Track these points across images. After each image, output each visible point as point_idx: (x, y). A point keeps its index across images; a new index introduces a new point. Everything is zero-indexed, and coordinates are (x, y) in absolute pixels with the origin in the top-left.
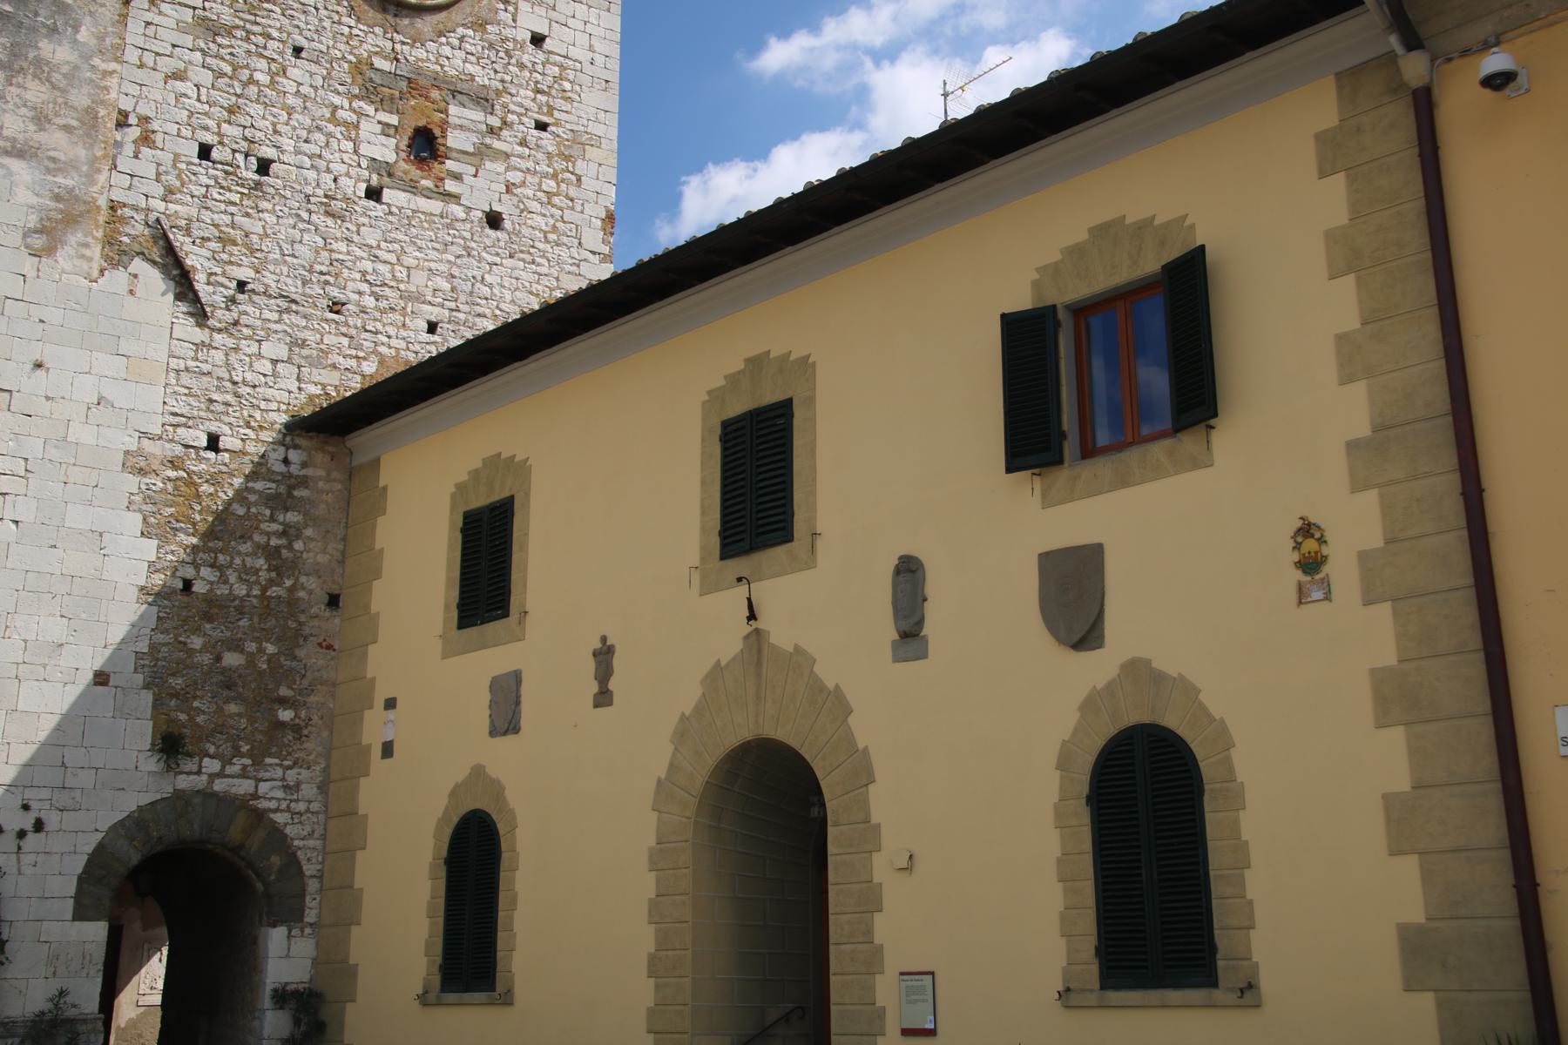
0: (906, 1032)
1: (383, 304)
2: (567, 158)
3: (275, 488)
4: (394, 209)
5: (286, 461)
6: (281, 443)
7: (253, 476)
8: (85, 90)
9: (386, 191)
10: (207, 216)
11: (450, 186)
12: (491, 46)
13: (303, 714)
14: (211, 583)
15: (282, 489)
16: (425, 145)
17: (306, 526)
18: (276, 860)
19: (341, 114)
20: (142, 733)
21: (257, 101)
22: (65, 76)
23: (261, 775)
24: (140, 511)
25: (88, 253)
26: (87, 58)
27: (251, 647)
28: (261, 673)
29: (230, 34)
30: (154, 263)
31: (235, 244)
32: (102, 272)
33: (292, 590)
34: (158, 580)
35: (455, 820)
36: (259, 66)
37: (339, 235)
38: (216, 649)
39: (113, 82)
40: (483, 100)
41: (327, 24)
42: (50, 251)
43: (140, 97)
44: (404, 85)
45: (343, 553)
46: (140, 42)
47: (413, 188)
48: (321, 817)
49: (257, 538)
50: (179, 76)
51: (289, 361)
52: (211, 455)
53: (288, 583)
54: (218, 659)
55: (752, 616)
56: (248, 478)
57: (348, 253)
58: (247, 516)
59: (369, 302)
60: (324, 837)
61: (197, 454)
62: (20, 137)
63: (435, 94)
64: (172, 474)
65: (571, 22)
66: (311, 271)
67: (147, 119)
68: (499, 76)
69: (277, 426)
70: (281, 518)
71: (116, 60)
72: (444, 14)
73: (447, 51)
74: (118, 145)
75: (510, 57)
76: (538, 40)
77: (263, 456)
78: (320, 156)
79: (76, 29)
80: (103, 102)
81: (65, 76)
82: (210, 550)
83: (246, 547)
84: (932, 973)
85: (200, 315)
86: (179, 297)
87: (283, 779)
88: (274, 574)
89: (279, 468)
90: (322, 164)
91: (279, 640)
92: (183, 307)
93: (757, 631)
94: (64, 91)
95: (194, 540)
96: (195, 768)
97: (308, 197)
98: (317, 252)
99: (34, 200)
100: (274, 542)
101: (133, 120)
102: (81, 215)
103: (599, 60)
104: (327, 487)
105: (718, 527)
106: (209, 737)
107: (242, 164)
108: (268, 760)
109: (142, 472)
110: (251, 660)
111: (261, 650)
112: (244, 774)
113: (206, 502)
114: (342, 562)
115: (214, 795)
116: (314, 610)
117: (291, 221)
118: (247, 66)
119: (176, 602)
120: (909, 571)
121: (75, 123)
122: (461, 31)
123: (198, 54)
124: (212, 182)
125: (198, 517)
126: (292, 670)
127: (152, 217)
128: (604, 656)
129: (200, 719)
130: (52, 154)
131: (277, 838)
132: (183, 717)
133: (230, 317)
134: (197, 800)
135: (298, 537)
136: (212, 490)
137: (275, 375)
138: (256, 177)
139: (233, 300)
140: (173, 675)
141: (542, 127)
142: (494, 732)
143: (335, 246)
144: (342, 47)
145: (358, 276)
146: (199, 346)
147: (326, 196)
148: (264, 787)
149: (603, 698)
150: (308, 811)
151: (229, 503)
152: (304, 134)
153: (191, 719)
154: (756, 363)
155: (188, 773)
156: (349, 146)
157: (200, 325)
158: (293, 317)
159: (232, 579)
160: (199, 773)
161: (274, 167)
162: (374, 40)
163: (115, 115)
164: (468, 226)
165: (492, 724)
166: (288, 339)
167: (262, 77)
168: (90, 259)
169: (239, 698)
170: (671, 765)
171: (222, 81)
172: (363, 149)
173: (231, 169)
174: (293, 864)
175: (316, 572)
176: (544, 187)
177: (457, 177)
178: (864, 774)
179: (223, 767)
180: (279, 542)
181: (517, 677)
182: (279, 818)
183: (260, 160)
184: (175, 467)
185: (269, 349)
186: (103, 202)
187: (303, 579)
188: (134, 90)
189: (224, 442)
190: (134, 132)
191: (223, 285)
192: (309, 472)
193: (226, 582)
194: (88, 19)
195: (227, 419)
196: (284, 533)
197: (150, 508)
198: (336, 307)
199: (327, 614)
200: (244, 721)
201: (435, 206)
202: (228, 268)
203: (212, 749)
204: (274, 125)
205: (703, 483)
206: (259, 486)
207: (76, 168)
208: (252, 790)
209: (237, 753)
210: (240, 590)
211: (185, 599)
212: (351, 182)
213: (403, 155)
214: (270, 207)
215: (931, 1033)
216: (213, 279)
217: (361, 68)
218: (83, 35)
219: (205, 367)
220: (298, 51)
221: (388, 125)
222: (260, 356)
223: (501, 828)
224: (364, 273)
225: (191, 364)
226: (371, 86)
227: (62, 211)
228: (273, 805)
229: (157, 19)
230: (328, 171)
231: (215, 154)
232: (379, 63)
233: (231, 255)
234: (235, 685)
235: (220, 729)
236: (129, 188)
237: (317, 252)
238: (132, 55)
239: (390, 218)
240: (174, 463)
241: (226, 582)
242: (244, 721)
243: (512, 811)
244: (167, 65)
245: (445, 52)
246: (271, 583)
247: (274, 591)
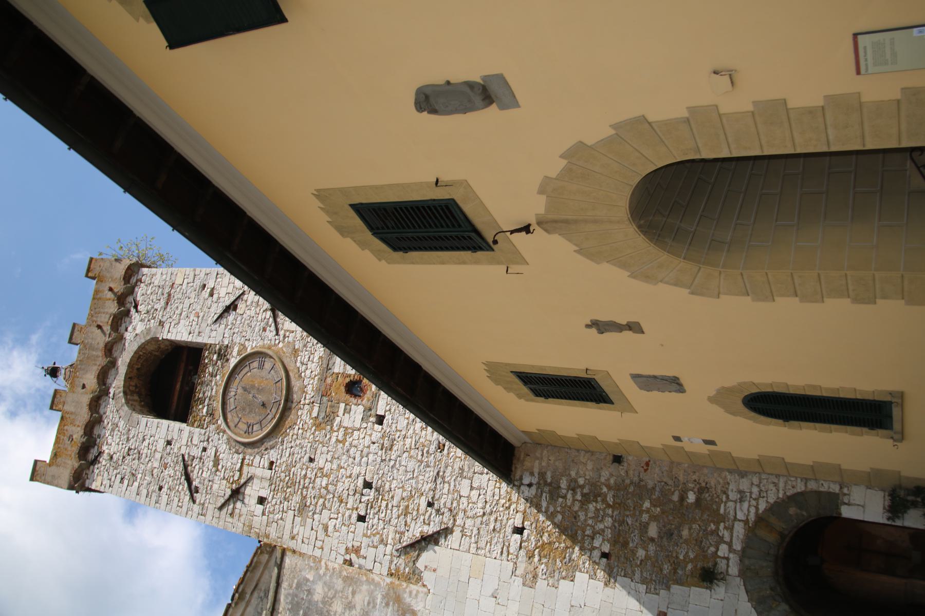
3: (546, 494)
4: (388, 408)
5: (530, 485)
6: (519, 487)
7: (538, 507)
9: (379, 413)
10: (394, 521)
12: (305, 346)
13: (691, 485)
14: (604, 540)
15: (546, 489)
17: (570, 475)
18: (792, 511)
19: (340, 438)
20: (699, 595)
21: (336, 485)
23: (732, 517)
24: (558, 580)
25: (414, 592)
26: (320, 577)
27: (645, 517)
28: (663, 512)
29: (305, 497)
30: (419, 555)
31: (407, 507)
32: (424, 586)
33: (609, 487)
34: (600, 574)
36: (319, 483)
37: (402, 443)
38: (647, 541)
41: (298, 442)
44: (325, 399)
45: (587, 452)
48: (764, 476)
50: (326, 528)
51: (471, 479)
52: (526, 532)
53: (605, 490)
54: (652, 540)
55: (527, 229)
56: (539, 511)
57: (411, 437)
58: (563, 513)
60: (778, 476)
61: (525, 541)
63: (329, 380)
64: (536, 559)
66: (421, 462)
67: (347, 549)
69: (509, 489)
70: (564, 491)
71: (320, 561)
72: (291, 374)
73: (308, 372)
74: (360, 567)
77: (526, 500)
79: (308, 580)
80: (340, 572)
82: (583, 539)
83: (582, 516)
84: (855, 35)
85: (446, 532)
87: (735, 502)
88: (599, 499)
89: (533, 490)
90: (366, 450)
91: (641, 498)
92: (442, 541)
93: (539, 223)
94: (336, 592)
95: (577, 549)
96: (725, 562)
97: (382, 460)
98: (411, 457)
100: (579, 497)
101: (348, 557)
104: (545, 459)
105: (470, 252)
106: (704, 551)
107: (367, 498)
108: (722, 511)
109: (535, 577)
110: (653, 518)
111: (648, 511)
112: (731, 529)
113: (553, 539)
114: (593, 453)
115: (743, 550)
116: (623, 473)
117: (395, 471)
119: (616, 563)
120: (429, 100)
121: (351, 589)
122: (298, 364)
123: (315, 516)
125: (563, 545)
126: (661, 491)
127: (395, 553)
128: (600, 326)
129: (692, 555)
131: (776, 508)
132: (690, 567)
133: (447, 514)
134: (747, 562)
135: (576, 481)
136: (546, 534)
137: (479, 488)
139: (438, 511)
140: (661, 570)
143: (408, 446)
144: (308, 434)
145: (424, 432)
148: (740, 516)
149: (634, 327)
150: (758, 486)
151: (554, 524)
152: (351, 460)
153: (691, 561)
154: (343, 231)
155: (728, 566)
157: (452, 532)
158: (447, 474)
159: (601, 526)
160: (728, 559)
162: (305, 415)
163: (346, 567)
166: (459, 479)
168: (418, 592)
169: (679, 528)
170: (676, 285)
173: (369, 505)
174: (796, 499)
175: (598, 470)
178: (638, 127)
179: (725, 542)
180: (579, 493)
181: (635, 377)
182: (762, 506)
183: (365, 487)
184: (533, 556)
185: (465, 491)
186: (389, 580)
187: (603, 480)
188: (334, 554)
190: (353, 557)
191: (430, 516)
192: (536, 471)
193: (603, 531)
194: (303, 573)
195: (505, 521)
196: (573, 490)
197: (556, 574)
199: (625, 464)
200: (694, 526)
202: (421, 512)
203: (712, 549)
204: (347, 477)
205: (443, 263)
206: (544, 504)
208: (742, 524)
209: (715, 532)
210: (609, 521)
211: (613, 558)
212: (374, 434)
213: (359, 401)
214: (388, 484)
216: (427, 522)
218: (310, 577)
219: (475, 532)
220: (311, 460)
221: (345, 409)
223: (755, 390)
225: (473, 540)
226: (326, 420)
228: (753, 510)
229: (300, 537)
230: (369, 447)
231: (362, 513)
232: (315, 414)
233: (413, 509)
234: (670, 530)
237: (411, 457)
238: (318, 553)
240: (530, 557)
241: (603, 531)
242: (694, 526)
243: (740, 384)
244: (321, 534)
246: (604, 501)
247: (610, 500)
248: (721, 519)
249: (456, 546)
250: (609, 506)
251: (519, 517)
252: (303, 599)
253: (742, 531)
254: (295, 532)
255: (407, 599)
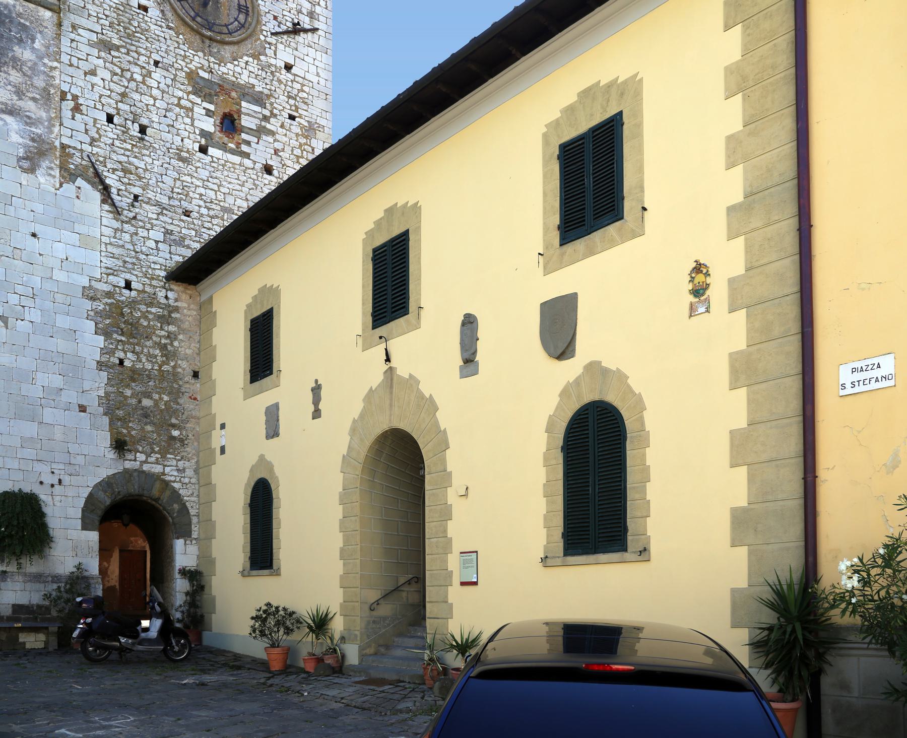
0: (463, 584)
1: (212, 213)
2: (306, 137)
5: (166, 297)
8: (42, 77)
10: (114, 156)
11: (244, 148)
16: (230, 123)
21: (137, 91)
22: (30, 68)
23: (165, 463)
25: (53, 173)
26: (41, 58)
27: (156, 396)
28: (162, 411)
35: (253, 484)
39: (56, 73)
40: (259, 100)
42: (32, 170)
43: (72, 83)
46: (69, 50)
47: (224, 147)
49: (154, 338)
50: (93, 73)
51: (164, 242)
54: (140, 402)
58: (148, 326)
59: (204, 211)
62: (9, 102)
64: (109, 301)
65: (306, 58)
68: (268, 87)
71: (56, 60)
75: (274, 76)
76: (288, 67)
78: (173, 126)
79: (33, 41)
80: (52, 85)
81: (30, 68)
85: (117, 212)
86: (104, 201)
92: (106, 207)
99: (21, 140)
101: (69, 97)
102: (47, 151)
103: (322, 82)
106: (139, 441)
108: (169, 456)
109: (93, 299)
110: (156, 403)
111: (161, 399)
112: (157, 462)
118: (129, 70)
121: (38, 97)
124: (116, 137)
129: (133, 433)
130: (27, 114)
133: (131, 215)
137: (158, 249)
138: (139, 135)
141: (292, 118)
142: (268, 437)
145: (198, 196)
146: (116, 230)
147: (178, 149)
148: (167, 469)
156: (188, 121)
159: (144, 360)
161: (149, 131)
164: (255, 172)
165: (267, 433)
166: (163, 230)
167: (139, 78)
168: (54, 177)
169: (152, 423)
171: (115, 78)
172: (196, 123)
176: (295, 153)
177: (248, 143)
182: (176, 485)
183: (140, 125)
186: (57, 144)
188: (69, 80)
189: (134, 285)
194: (39, 36)
198: (187, 213)
201: (236, 159)
203: (140, 449)
206: (153, 310)
207: (42, 123)
208: (162, 471)
209: (153, 451)
210: (149, 366)
211: (121, 369)
213: (218, 128)
214: (148, 153)
215: (475, 583)
217: (192, 76)
218: (37, 45)
219: (121, 243)
220: (156, 63)
222: (149, 238)
224: (201, 195)
227: (36, 148)
228: (172, 478)
229: (77, 38)
231: (116, 120)
235: (144, 438)
236: (71, 137)
238: (65, 58)
239: (213, 164)
240: (109, 294)
241: (140, 361)
245: (242, 71)
248: (163, 454)
249: (105, 221)
250: (160, 366)
251: (140, 287)
252: (10, 31)
253: (157, 471)
254: (80, 31)
255: (45, 164)
